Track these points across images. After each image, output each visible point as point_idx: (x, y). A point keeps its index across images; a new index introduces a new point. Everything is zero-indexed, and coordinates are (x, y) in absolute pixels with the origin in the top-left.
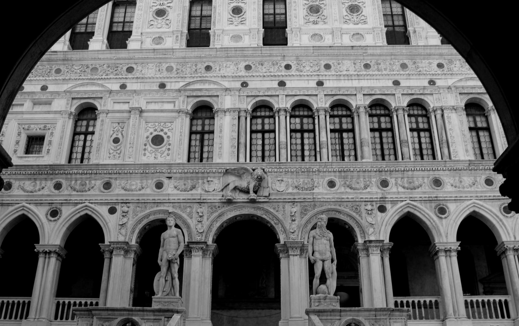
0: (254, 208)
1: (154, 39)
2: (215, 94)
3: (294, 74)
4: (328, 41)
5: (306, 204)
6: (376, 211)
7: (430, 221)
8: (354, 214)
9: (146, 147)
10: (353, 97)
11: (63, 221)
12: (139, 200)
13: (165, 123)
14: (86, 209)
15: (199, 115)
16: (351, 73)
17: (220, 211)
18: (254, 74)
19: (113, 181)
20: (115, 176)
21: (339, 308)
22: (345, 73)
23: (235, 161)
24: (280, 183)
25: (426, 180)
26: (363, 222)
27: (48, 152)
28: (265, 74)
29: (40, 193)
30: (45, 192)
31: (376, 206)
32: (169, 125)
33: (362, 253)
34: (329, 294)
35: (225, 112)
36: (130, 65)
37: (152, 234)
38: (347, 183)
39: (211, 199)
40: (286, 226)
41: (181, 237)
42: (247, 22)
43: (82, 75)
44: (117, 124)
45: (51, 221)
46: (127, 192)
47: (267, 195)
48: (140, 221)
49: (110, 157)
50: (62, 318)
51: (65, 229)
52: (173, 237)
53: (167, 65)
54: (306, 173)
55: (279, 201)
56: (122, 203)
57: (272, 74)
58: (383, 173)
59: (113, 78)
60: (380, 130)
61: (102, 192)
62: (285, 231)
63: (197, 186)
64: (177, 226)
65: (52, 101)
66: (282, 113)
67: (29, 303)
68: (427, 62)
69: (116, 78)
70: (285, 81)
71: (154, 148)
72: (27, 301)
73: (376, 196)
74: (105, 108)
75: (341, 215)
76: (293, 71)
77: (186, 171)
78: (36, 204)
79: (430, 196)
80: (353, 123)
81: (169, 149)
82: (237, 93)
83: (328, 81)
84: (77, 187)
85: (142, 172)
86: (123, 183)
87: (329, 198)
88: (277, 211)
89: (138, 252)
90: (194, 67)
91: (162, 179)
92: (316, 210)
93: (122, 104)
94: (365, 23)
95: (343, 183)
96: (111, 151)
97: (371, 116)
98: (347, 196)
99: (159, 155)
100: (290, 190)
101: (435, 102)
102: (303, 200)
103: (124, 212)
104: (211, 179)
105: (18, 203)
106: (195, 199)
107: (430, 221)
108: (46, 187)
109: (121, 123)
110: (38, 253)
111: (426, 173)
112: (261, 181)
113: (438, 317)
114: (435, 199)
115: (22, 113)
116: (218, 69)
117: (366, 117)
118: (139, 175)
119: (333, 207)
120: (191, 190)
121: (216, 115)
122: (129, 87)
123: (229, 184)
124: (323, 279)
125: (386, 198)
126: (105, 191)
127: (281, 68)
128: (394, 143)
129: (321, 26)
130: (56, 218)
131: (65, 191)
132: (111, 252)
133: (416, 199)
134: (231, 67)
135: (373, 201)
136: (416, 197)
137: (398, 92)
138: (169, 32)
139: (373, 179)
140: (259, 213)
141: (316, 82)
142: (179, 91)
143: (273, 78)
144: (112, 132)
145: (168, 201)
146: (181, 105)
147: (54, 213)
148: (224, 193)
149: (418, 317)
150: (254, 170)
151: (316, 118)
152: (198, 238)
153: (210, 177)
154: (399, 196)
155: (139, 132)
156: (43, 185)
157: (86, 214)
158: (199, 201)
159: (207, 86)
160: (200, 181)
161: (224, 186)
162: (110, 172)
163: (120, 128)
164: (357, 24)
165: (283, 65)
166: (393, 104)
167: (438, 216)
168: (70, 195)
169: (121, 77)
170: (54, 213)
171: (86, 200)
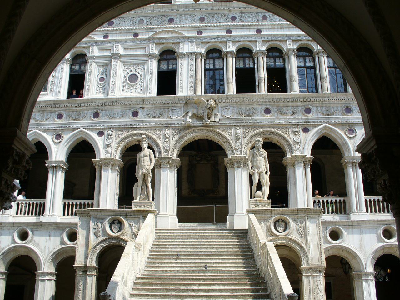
6: (301, 132)
8: (284, 135)
9: (124, 84)
10: (284, 43)
11: (66, 142)
12: (120, 125)
14: (82, 134)
15: (165, 57)
18: (207, 25)
19: (100, 112)
20: (102, 107)
21: (271, 209)
24: (228, 111)
25: (339, 108)
26: (291, 141)
27: (51, 90)
28: (215, 24)
31: (301, 129)
33: (290, 164)
34: (263, 198)
37: (132, 152)
39: (174, 124)
41: (153, 156)
45: (56, 143)
50: (68, 215)
51: (66, 148)
52: (146, 156)
53: (139, 19)
55: (227, 125)
56: (107, 128)
57: (221, 24)
62: (231, 148)
63: (164, 113)
64: (150, 147)
66: (229, 55)
67: (44, 204)
70: (231, 30)
72: (42, 203)
74: (92, 55)
78: (45, 131)
79: (342, 120)
80: (284, 62)
83: (265, 29)
85: (122, 104)
87: (266, 123)
89: (121, 165)
92: (255, 131)
96: (98, 88)
97: (298, 56)
99: (135, 90)
100: (235, 117)
104: (175, 108)
105: (32, 130)
111: (340, 103)
112: (213, 110)
114: (346, 123)
116: (178, 20)
118: (119, 107)
119: (269, 129)
120: (159, 117)
123: (188, 112)
124: (259, 187)
125: (309, 122)
127: (228, 20)
130: (60, 141)
132: (101, 167)
133: (331, 123)
135: (299, 125)
136: (332, 122)
141: (255, 30)
142: (149, 39)
143: (222, 28)
147: (59, 136)
149: (330, 212)
153: (174, 107)
156: (49, 116)
159: (170, 35)
160: (166, 110)
161: (186, 112)
162: (98, 105)
163: (104, 70)
165: (230, 16)
167: (348, 136)
170: (59, 136)
171: (80, 126)
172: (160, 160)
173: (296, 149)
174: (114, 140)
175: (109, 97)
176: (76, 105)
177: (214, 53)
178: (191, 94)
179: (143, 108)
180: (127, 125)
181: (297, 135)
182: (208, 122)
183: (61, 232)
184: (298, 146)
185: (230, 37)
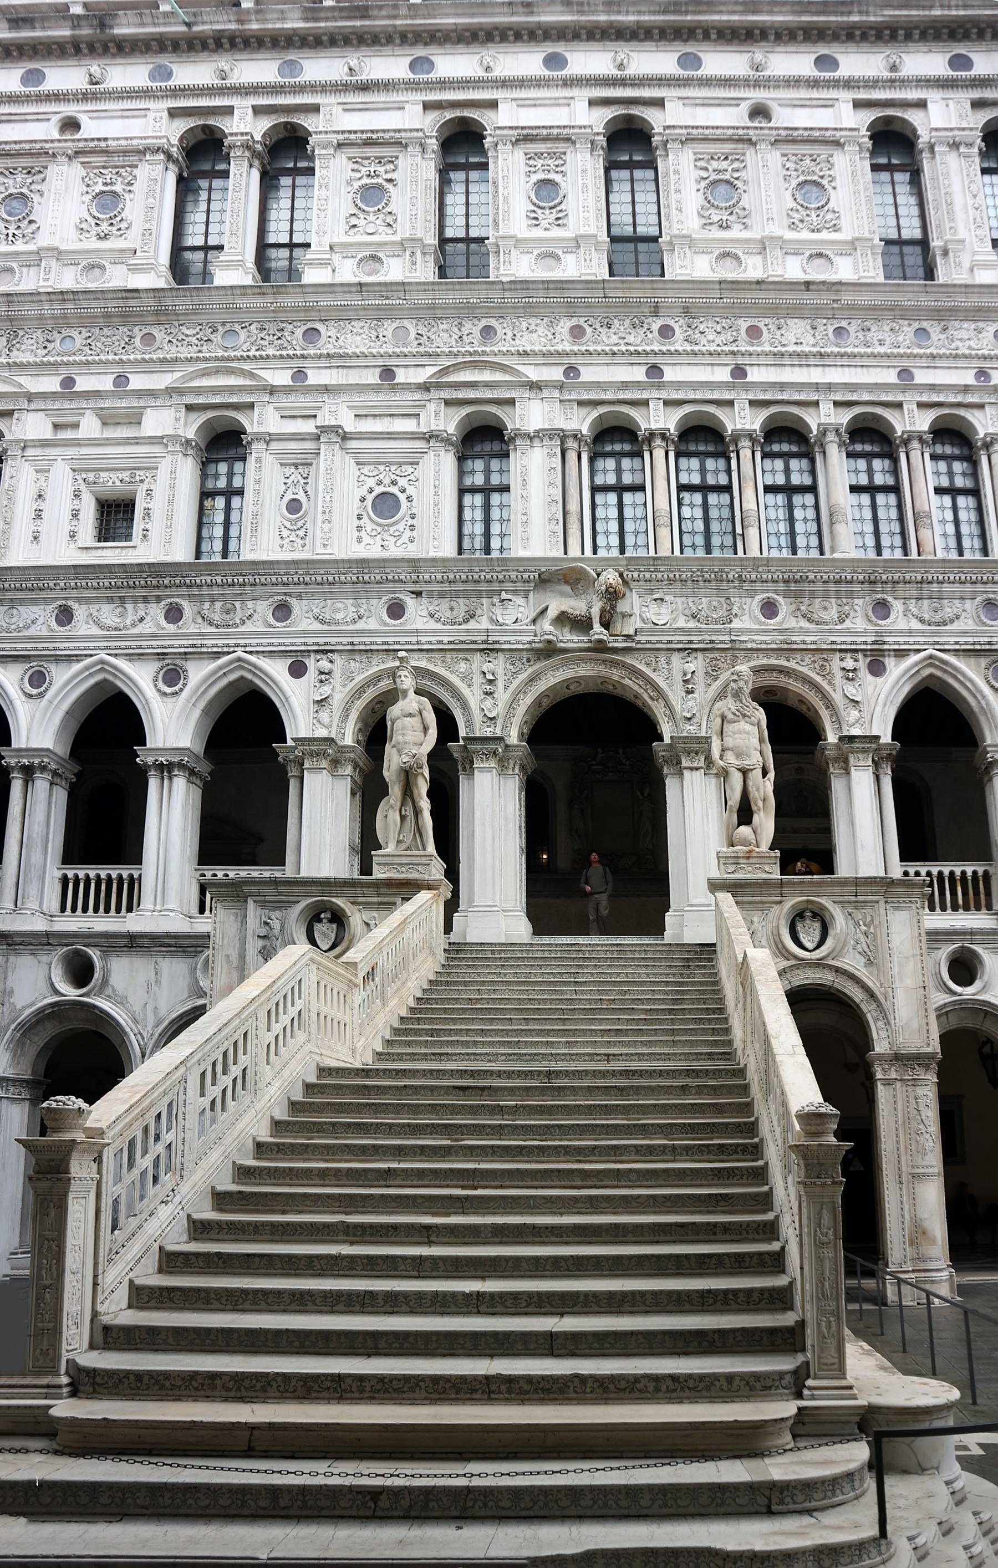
0: (605, 662)
1: (361, 260)
2: (507, 395)
3: (680, 349)
4: (753, 269)
5: (716, 655)
6: (864, 674)
7: (975, 697)
8: (818, 679)
10: (812, 410)
12: (352, 644)
13: (400, 464)
14: (241, 667)
16: (807, 349)
17: (530, 670)
19: (293, 602)
22: (791, 348)
23: (559, 553)
26: (837, 698)
27: (145, 536)
28: (615, 349)
29: (135, 631)
30: (147, 628)
31: (863, 663)
32: (410, 469)
35: (531, 439)
36: (310, 325)
38: (803, 608)
39: (509, 642)
40: (674, 703)
42: (571, 221)
43: (205, 348)
44: (293, 470)
45: (165, 694)
46: (325, 627)
47: (632, 632)
48: (360, 691)
49: (282, 547)
51: (197, 712)
53: (395, 325)
54: (713, 583)
56: (316, 652)
57: (632, 349)
58: (879, 587)
59: (275, 356)
60: (872, 489)
61: (271, 626)
62: (672, 715)
63: (479, 612)
65: (142, 414)
66: (658, 442)
68: (973, 327)
69: (281, 356)
71: (380, 525)
73: (863, 639)
74: (262, 430)
75: (791, 681)
76: (678, 343)
77: (451, 576)
78: (130, 657)
81: (412, 527)
82: (556, 394)
83: (756, 368)
84: (217, 617)
85: (354, 578)
86: (316, 606)
88: (655, 670)
90: (456, 330)
91: (401, 596)
93: (300, 420)
94: (835, 228)
95: (793, 607)
96: (285, 533)
98: (801, 638)
99: (393, 540)
100: (681, 623)
101: (990, 423)
102: (709, 646)
103: (322, 673)
104: (509, 597)
105: (91, 656)
106: (474, 642)
107: (975, 697)
108: (148, 618)
109: (304, 463)
110: (145, 764)
113: (989, 908)
114: (987, 647)
115: (77, 443)
116: (510, 334)
117: (841, 457)
118: (348, 588)
120: (466, 621)
121: (511, 447)
122: (315, 377)
123: (546, 609)
125: (884, 643)
126: (278, 624)
127: (650, 336)
128: (901, 519)
129: (736, 232)
130: (176, 688)
131: (190, 624)
133: (947, 647)
134: (541, 331)
135: (856, 651)
137: (910, 399)
138: (393, 243)
139: (856, 601)
140: (615, 674)
141: (729, 369)
142: (425, 387)
143: (635, 359)
144: (284, 487)
145: (416, 647)
146: (433, 421)
147: (173, 676)
148: (537, 628)
150: (598, 575)
151: (733, 455)
152: (488, 732)
154: (911, 640)
155: (343, 485)
157: (242, 678)
158: (485, 646)
159: (487, 376)
161: (538, 610)
162: (285, 579)
164: (819, 231)
165: (656, 325)
166: (900, 424)
168: (201, 634)
169: (291, 352)
170: (173, 676)
171: (237, 645)
172: (472, 747)
173: (852, 720)
174: (338, 688)
175: (316, 557)
176: (219, 581)
177: (616, 436)
178: (559, 553)
179: (418, 594)
180: (372, 643)
181: (853, 679)
182: (601, 637)
183: (190, 960)
184: (856, 712)
185: (660, 386)
